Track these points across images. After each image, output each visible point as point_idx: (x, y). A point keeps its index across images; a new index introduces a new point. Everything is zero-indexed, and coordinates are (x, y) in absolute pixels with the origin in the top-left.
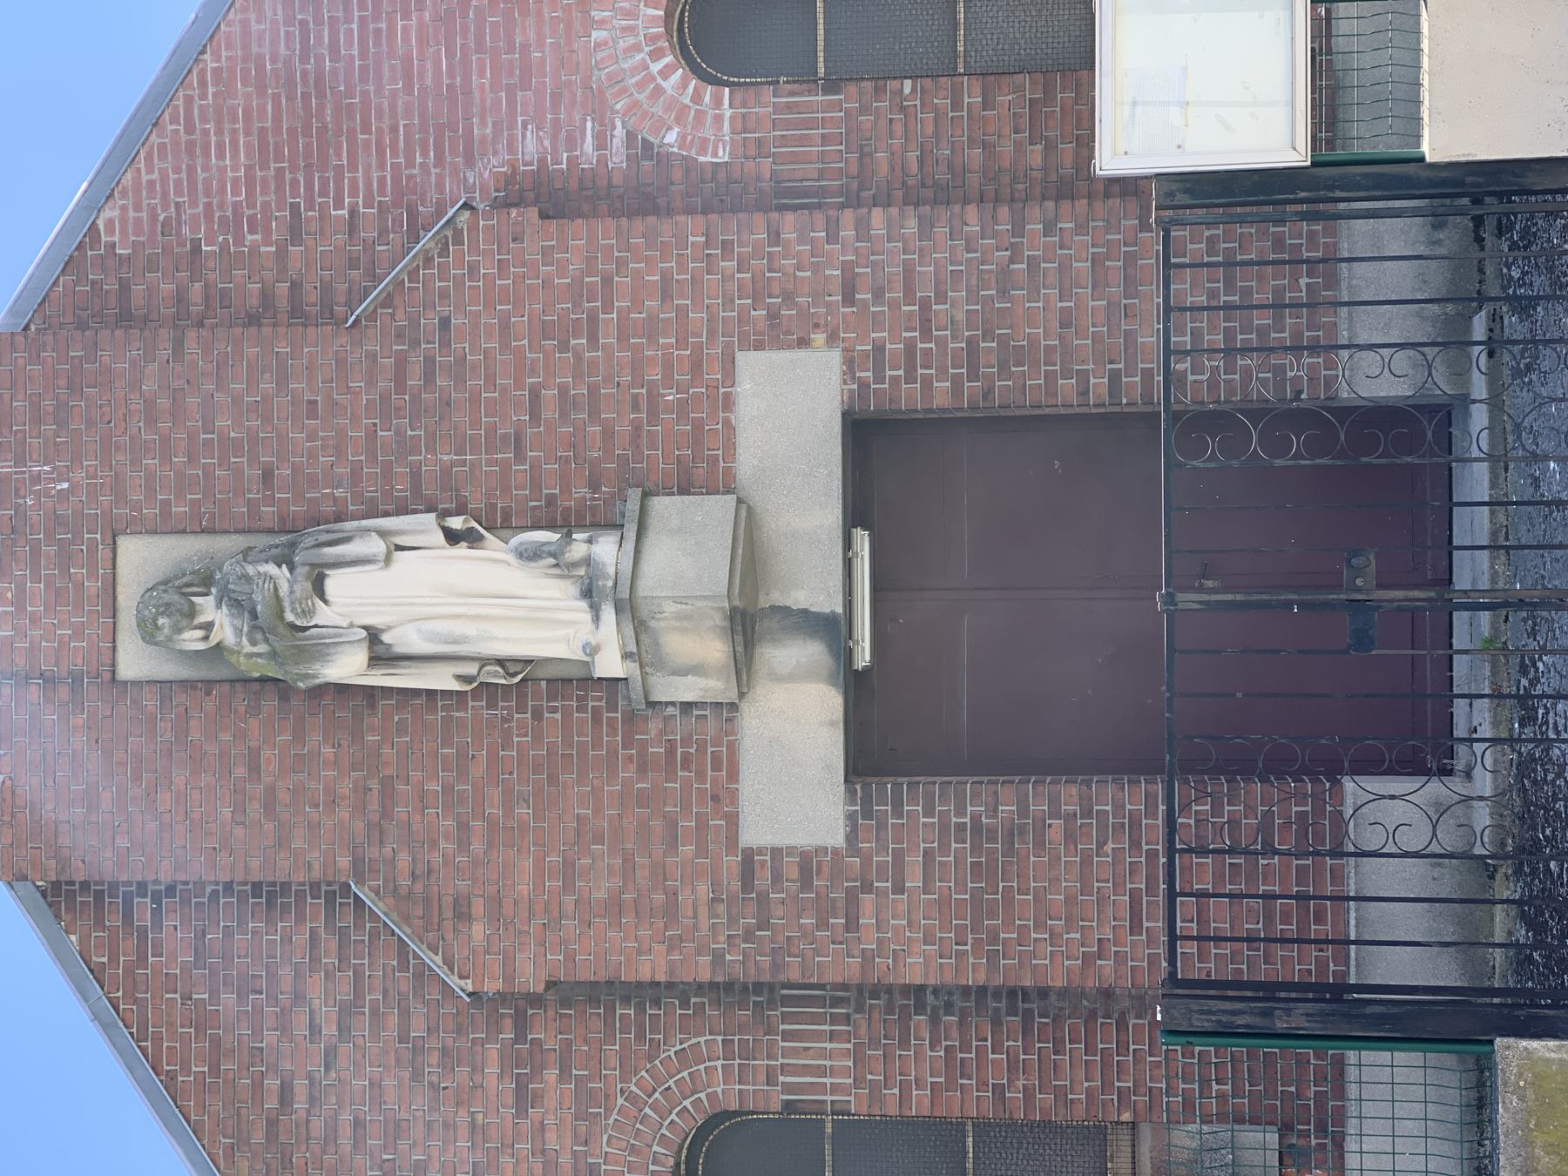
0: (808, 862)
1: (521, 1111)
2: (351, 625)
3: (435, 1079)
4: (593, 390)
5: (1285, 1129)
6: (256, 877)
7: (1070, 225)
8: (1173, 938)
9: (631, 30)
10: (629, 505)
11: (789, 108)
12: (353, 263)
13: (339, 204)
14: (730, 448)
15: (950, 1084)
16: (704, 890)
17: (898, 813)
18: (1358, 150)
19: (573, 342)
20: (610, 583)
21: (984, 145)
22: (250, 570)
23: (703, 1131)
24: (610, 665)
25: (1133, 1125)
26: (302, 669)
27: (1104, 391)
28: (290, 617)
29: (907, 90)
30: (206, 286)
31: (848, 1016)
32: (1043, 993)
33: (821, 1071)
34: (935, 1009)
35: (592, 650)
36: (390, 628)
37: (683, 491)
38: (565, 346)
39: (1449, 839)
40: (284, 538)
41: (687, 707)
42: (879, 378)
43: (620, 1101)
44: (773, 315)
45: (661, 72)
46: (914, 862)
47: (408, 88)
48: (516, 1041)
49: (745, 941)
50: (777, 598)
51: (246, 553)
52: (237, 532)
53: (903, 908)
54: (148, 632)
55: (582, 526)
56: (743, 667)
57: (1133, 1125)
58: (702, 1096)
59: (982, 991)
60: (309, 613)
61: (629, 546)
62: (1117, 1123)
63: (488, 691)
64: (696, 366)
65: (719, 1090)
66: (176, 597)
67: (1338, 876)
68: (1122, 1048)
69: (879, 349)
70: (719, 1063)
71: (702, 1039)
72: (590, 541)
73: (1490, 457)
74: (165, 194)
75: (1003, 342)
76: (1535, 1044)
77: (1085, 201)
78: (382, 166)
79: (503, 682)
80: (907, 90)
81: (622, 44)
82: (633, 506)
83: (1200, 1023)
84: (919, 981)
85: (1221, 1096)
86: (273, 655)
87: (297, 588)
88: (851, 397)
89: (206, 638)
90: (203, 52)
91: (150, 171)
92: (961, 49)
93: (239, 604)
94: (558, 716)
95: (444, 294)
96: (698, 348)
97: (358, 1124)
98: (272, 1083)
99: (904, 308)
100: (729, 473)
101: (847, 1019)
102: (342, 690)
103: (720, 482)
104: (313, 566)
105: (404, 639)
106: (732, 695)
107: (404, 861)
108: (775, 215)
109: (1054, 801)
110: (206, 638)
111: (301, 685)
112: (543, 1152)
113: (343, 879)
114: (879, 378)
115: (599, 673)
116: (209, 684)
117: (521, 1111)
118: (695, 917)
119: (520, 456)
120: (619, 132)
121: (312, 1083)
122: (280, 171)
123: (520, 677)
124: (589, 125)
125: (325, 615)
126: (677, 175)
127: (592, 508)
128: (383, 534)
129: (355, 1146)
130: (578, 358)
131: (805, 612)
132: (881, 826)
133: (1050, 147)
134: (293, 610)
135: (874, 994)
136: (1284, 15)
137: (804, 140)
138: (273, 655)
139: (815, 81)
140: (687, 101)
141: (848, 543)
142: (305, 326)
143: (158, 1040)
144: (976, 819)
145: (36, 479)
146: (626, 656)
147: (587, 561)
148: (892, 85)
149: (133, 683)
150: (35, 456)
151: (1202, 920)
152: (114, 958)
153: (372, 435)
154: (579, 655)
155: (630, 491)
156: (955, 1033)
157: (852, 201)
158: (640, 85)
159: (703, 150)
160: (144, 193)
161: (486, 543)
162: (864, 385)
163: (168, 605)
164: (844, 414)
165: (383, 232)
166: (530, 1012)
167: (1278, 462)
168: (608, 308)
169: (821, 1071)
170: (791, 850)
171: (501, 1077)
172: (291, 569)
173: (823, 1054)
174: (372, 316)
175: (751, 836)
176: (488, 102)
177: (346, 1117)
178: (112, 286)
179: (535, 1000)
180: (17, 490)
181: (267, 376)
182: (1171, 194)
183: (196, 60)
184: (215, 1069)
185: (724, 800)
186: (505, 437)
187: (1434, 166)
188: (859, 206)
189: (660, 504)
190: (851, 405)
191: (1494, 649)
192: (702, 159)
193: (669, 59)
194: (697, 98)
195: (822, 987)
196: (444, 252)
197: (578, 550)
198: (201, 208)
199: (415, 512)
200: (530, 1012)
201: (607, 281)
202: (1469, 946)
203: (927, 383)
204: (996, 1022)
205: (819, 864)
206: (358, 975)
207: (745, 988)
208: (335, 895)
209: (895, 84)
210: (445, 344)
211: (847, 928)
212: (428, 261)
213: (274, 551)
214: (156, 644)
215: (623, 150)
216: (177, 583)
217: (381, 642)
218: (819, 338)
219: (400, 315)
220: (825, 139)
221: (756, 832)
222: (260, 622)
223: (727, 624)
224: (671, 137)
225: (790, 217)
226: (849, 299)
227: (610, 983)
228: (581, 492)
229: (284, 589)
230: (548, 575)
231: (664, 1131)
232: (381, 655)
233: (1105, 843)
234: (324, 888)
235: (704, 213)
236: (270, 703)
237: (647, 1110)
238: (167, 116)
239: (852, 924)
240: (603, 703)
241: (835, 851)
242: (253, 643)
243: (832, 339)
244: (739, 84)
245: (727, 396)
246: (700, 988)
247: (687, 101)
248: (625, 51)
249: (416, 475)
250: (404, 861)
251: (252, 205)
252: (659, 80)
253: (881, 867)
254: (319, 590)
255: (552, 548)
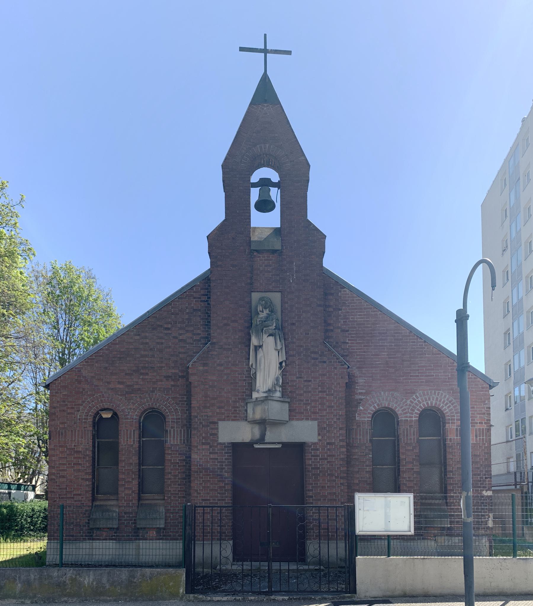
0: (216, 435)
1: (165, 377)
2: (263, 342)
3: (171, 359)
4: (310, 392)
5: (164, 529)
6: (211, 322)
7: (342, 488)
8: (204, 507)
9: (383, 400)
10: (287, 399)
11: (367, 432)
12: (337, 343)
13: (349, 340)
14: (298, 420)
15: (172, 463)
16: (210, 414)
17: (225, 453)
18: (359, 544)
19: (320, 388)
20: (271, 395)
21: (358, 471)
22: (274, 320)
23: (161, 414)
24: (255, 395)
25: (164, 499)
26: (254, 331)
27: (309, 495)
28: (265, 329)
29: (370, 456)
30: (332, 312)
31: (185, 443)
32: (190, 482)
33: (174, 437)
34: (186, 460)
35: (258, 391)
36: (262, 350)
37: (289, 410)
38: (319, 386)
39: (223, 561)
40: (280, 327)
41: (246, 411)
42: (312, 450)
43: (167, 397)
44: (325, 428)
45: (375, 406)
46: (216, 456)
47: (372, 355)
48: (179, 376)
49: (200, 422)
50: (268, 429)
51: (277, 320)
52: (282, 317)
53: (206, 454)
54: (262, 299)
55: (282, 389)
56: (254, 422)
57: (164, 499)
58: (169, 414)
59: (190, 470)
60: (265, 333)
61: (279, 399)
62: (165, 496)
63: (249, 370)
64: (315, 413)
65: (170, 417)
66: (269, 305)
67: (208, 540)
68: (179, 497)
69: (318, 450)
70: (175, 417)
71: (180, 414)
72: (280, 391)
73: (298, 569)
74: (351, 303)
75: (319, 475)
76: (184, 576)
77: (347, 491)
78: (357, 349)
79: (251, 373)
80: (370, 456)
81: (380, 398)
82: (287, 400)
83: (187, 512)
84: (192, 457)
85: (170, 516)
86: (257, 325)
87: (271, 330)
88: (308, 444)
89: (260, 311)
90: (381, 311)
91: (356, 300)
92: (378, 467)
93: (267, 318)
94: (244, 385)
95: (331, 362)
96: (318, 413)
97: (162, 343)
98: (170, 326)
99: (326, 455)
100: (293, 419)
101: (184, 443)
102: (250, 340)
103: (291, 418)
104: (275, 334)
105: (260, 354)
106: (249, 420)
107: (215, 353)
108: (345, 429)
109: (227, 484)
110: (260, 311)
111: (251, 331)
112: (157, 381)
113: (211, 340)
114: (312, 450)
115: (253, 393)
116: (251, 312)
117: (165, 377)
118: (204, 412)
119: (297, 378)
120: (363, 397)
121: (170, 334)
122: (355, 328)
123: (252, 377)
124: (364, 391)
125: (265, 336)
126: (353, 409)
127: (286, 391)
128: (281, 349)
129: (158, 343)
130: (316, 389)
131: (265, 434)
132: (223, 450)
133: (358, 484)
134: (266, 330)
135: (189, 448)
136: (384, 530)
137: (360, 435)
138: (257, 325)
139: (372, 437)
140: (368, 411)
141: (279, 443)
142: (324, 333)
143: (178, 301)
144: (224, 468)
145: (293, 275)
146: (257, 398)
147: (276, 391)
148: (371, 453)
149: (251, 296)
150: (297, 275)
151: (207, 513)
152: (195, 292)
153: (301, 346)
154: (257, 389)
155: (289, 399)
156: (182, 464)
157: (348, 445)
158: (372, 402)
159: (359, 414)
160: (351, 299)
161: (279, 370)
162: (310, 446)
163: (267, 303)
164: (304, 442)
165: (343, 349)
166: (185, 379)
167: (297, 528)
168: (327, 395)
169: (174, 437)
170: (218, 431)
171: (172, 373)
172: (274, 329)
173: (177, 437)
174: (326, 347)
175: (221, 423)
176: (370, 372)
177: (163, 341)
178: (332, 291)
179: (187, 380)
180: (290, 271)
181: (314, 324)
182: (351, 508)
183: (379, 310)
184: (172, 314)
185: (228, 418)
186: (301, 375)
187: (355, 559)
188: (347, 446)
189: (287, 405)
190: (306, 444)
191: (259, 570)
192: (357, 414)
193: (377, 407)
194: (369, 413)
195: (191, 437)
196: (339, 362)
197: (278, 389)
198: (348, 311)
199: (286, 355)
200: (185, 379)
201: (332, 395)
202: (203, 564)
203: (311, 459)
204: (184, 472)
205: (215, 437)
206: (192, 344)
207: (190, 422)
208: (208, 339)
209: (371, 454)
210: (320, 362)
211: (202, 443)
212: (337, 359)
213: (278, 325)
214: (259, 301)
215: (359, 398)
216: (271, 305)
217: (260, 348)
218: (320, 438)
219: (326, 353)
220: (360, 439)
221: (222, 425)
222: (264, 323)
223: (263, 419)
224: (361, 408)
225: (345, 432)
226: (328, 444)
227: (191, 395)
228: (290, 389)
229: (270, 328)
230: (273, 382)
231: (162, 406)
232: (257, 348)
233: (220, 494)
234: (209, 336)
235: (346, 415)
236: (247, 325)
237: (166, 402)
238: (367, 304)
239: (203, 444)
240: (247, 394)
241: (218, 440)
242: (259, 321)
243: (320, 440)
244: (372, 422)
245: (308, 419)
246: (190, 413)
247: (368, 411)
248: (379, 399)
249: (293, 356)
250: (215, 353)
251: (349, 321)
252: (373, 406)
253: (214, 450)
254: (270, 335)
255: (278, 383)
